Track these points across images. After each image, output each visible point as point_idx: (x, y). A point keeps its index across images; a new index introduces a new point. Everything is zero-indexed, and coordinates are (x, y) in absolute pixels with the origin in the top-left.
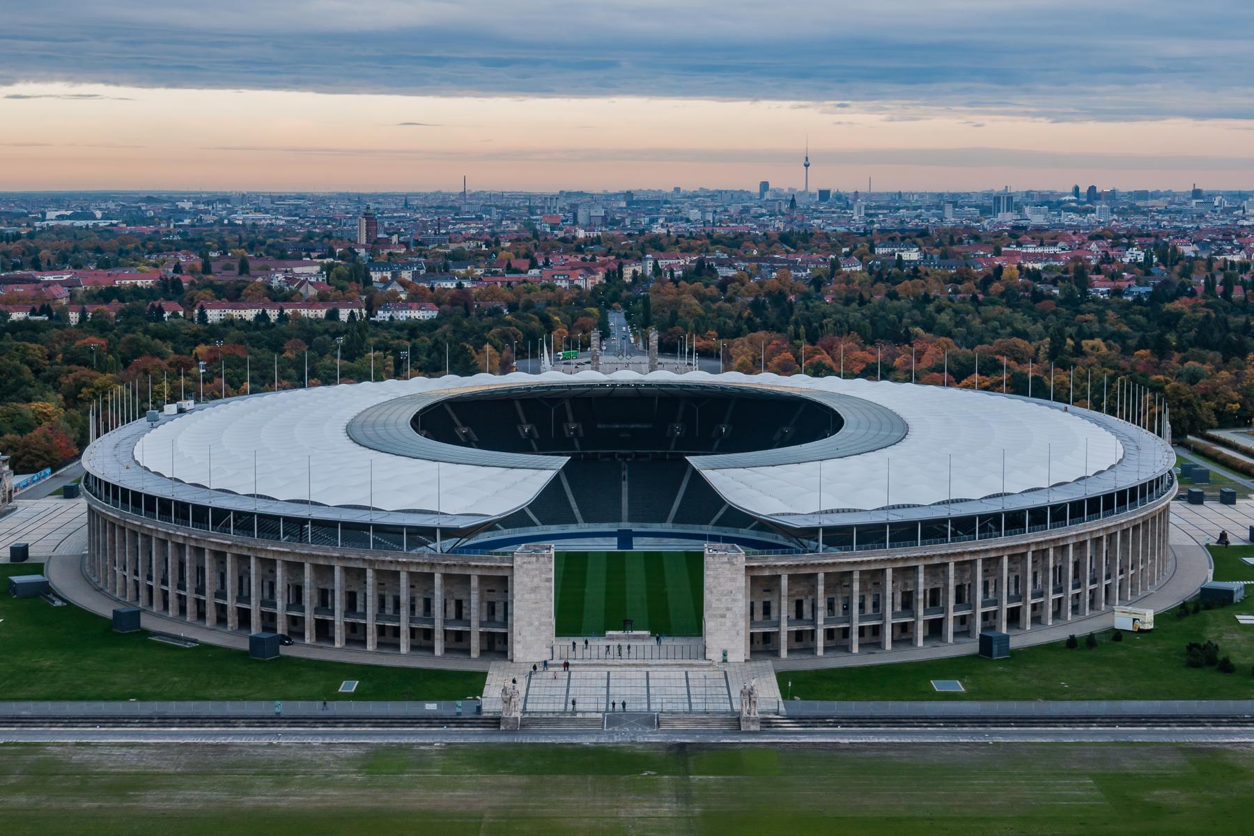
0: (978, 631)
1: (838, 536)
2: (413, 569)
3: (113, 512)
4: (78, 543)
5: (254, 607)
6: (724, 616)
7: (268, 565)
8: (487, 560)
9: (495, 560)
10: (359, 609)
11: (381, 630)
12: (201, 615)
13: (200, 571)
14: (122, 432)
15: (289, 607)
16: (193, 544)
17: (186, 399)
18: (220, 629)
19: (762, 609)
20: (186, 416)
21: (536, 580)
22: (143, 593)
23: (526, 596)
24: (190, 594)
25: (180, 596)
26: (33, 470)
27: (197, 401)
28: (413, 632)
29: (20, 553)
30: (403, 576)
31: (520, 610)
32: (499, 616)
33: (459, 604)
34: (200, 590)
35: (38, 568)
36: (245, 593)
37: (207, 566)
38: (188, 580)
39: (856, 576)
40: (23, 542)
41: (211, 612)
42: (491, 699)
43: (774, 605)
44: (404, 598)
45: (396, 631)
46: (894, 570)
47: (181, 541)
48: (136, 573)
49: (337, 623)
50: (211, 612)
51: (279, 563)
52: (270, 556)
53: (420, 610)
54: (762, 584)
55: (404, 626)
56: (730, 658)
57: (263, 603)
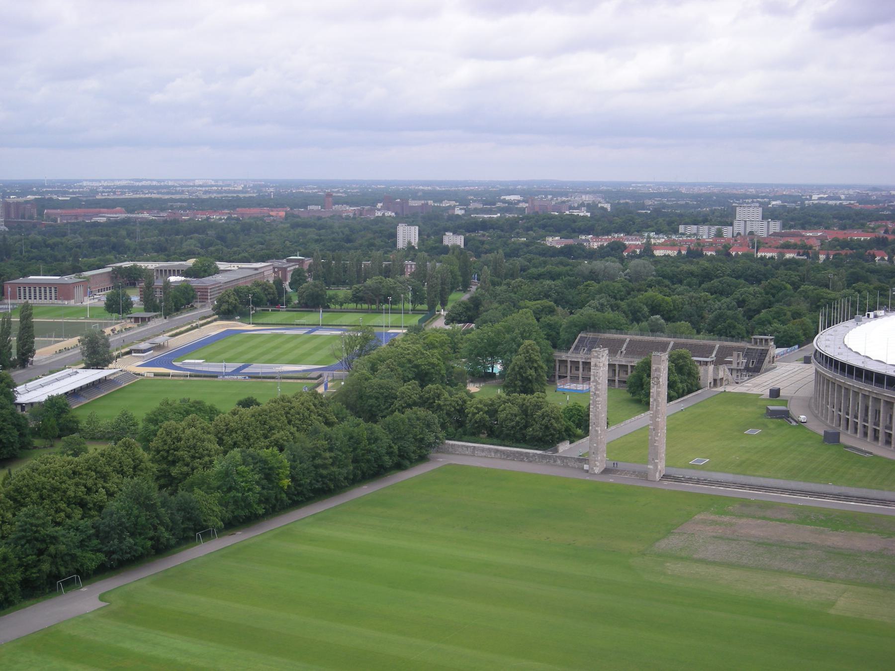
3: (829, 373)
4: (809, 390)
12: (876, 438)
13: (877, 412)
14: (839, 327)
17: (880, 309)
18: (887, 447)
20: (878, 320)
22: (843, 422)
24: (870, 425)
25: (865, 426)
26: (789, 346)
27: (886, 311)
29: (775, 393)
35: (785, 402)
37: (882, 410)
38: (870, 416)
40: (777, 387)
41: (881, 436)
48: (840, 411)
50: (881, 436)
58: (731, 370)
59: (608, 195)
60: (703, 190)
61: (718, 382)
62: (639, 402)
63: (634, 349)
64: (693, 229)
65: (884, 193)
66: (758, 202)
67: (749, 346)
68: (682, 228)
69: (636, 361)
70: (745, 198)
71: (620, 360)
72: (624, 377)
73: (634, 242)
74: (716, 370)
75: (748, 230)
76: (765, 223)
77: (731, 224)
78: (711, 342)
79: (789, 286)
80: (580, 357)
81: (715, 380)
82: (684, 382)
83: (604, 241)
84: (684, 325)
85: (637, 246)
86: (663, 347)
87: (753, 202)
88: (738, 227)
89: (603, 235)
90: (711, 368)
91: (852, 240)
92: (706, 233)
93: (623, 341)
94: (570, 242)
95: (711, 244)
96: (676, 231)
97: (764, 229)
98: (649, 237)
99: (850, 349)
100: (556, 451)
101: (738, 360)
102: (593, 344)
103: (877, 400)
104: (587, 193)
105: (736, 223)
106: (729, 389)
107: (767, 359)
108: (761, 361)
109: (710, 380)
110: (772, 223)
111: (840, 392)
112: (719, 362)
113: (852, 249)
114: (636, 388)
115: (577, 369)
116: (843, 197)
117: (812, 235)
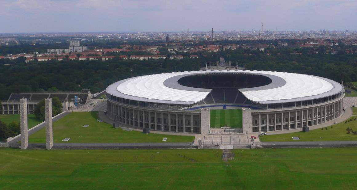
0: (302, 126)
1: (272, 106)
2: (179, 114)
3: (112, 101)
5: (144, 122)
6: (247, 124)
7: (146, 113)
8: (194, 111)
9: (197, 112)
10: (167, 122)
11: (172, 127)
13: (132, 115)
15: (151, 122)
16: (130, 108)
19: (255, 122)
21: (206, 116)
22: (119, 119)
23: (204, 119)
28: (178, 127)
30: (177, 115)
31: (202, 122)
32: (198, 124)
33: (189, 121)
34: (132, 118)
36: (142, 119)
39: (276, 115)
42: (196, 143)
43: (257, 121)
44: (177, 120)
45: (175, 127)
47: (127, 108)
49: (162, 126)
51: (149, 112)
52: (147, 111)
53: (180, 123)
54: (255, 116)
55: (177, 126)
56: (248, 133)
57: (146, 121)
58: (74, 103)
59: (17, 38)
60: (56, 35)
61: (70, 108)
63: (34, 98)
64: (53, 50)
65: (124, 35)
66: (77, 39)
67: (80, 93)
68: (48, 50)
70: (73, 38)
73: (29, 57)
74: (69, 104)
75: (75, 51)
76: (81, 47)
77: (68, 48)
78: (67, 93)
80: (13, 103)
81: (69, 108)
82: (57, 108)
83: (17, 56)
85: (31, 58)
86: (46, 96)
87: (75, 39)
88: (71, 49)
90: (67, 103)
91: (114, 52)
92: (58, 51)
95: (61, 56)
96: (46, 52)
97: (79, 49)
98: (36, 54)
99: (120, 92)
100: (6, 141)
102: (18, 98)
103: (131, 110)
104: (8, 37)
106: (74, 111)
107: (88, 98)
108: (86, 99)
110: (84, 47)
112: (70, 101)
113: (114, 55)
114: (38, 114)
115: (12, 108)
116: (109, 37)
117: (99, 51)
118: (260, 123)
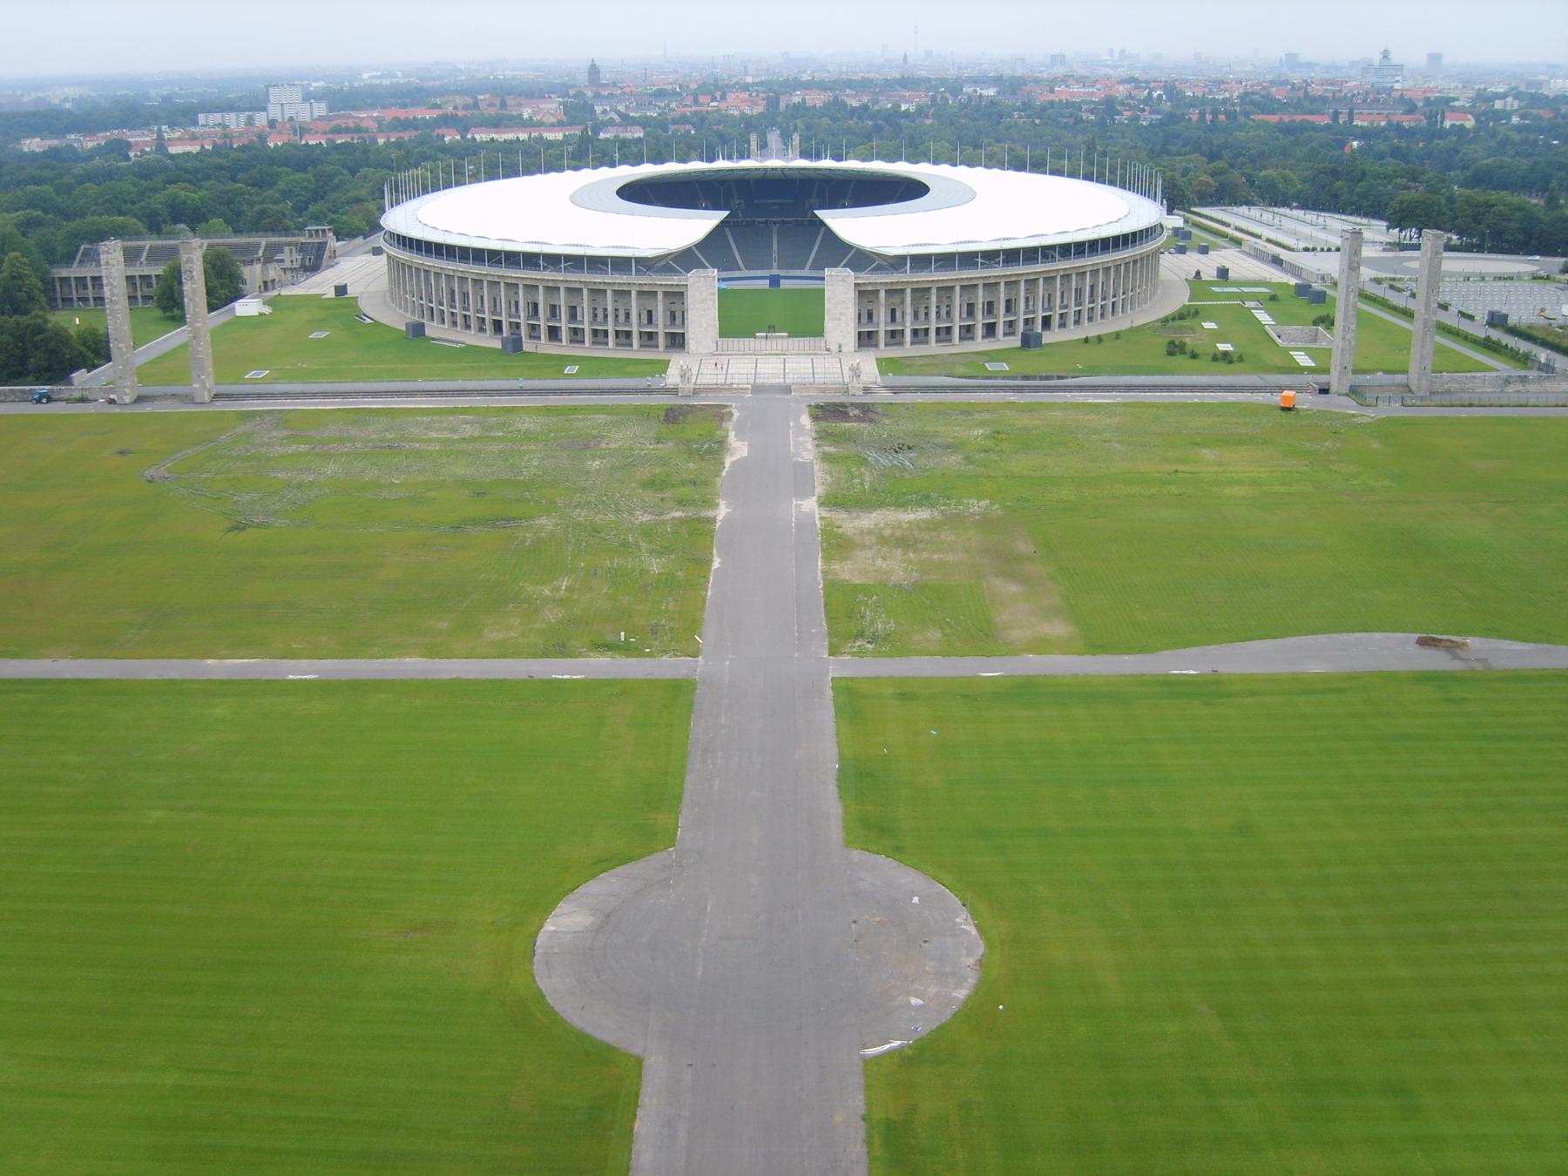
4: (383, 282)
13: (465, 296)
15: (529, 318)
28: (617, 333)
46: (962, 287)
62: (173, 319)
67: (303, 240)
68: (201, 118)
69: (159, 270)
71: (138, 271)
72: (148, 291)
75: (287, 117)
77: (265, 109)
79: (345, 172)
83: (101, 139)
84: (217, 222)
85: (146, 144)
89: (100, 130)
93: (141, 249)
94: (55, 142)
96: (195, 123)
101: (290, 257)
105: (270, 108)
106: (285, 292)
108: (319, 257)
109: (259, 282)
110: (315, 105)
111: (418, 276)
115: (85, 287)
118: (882, 318)
